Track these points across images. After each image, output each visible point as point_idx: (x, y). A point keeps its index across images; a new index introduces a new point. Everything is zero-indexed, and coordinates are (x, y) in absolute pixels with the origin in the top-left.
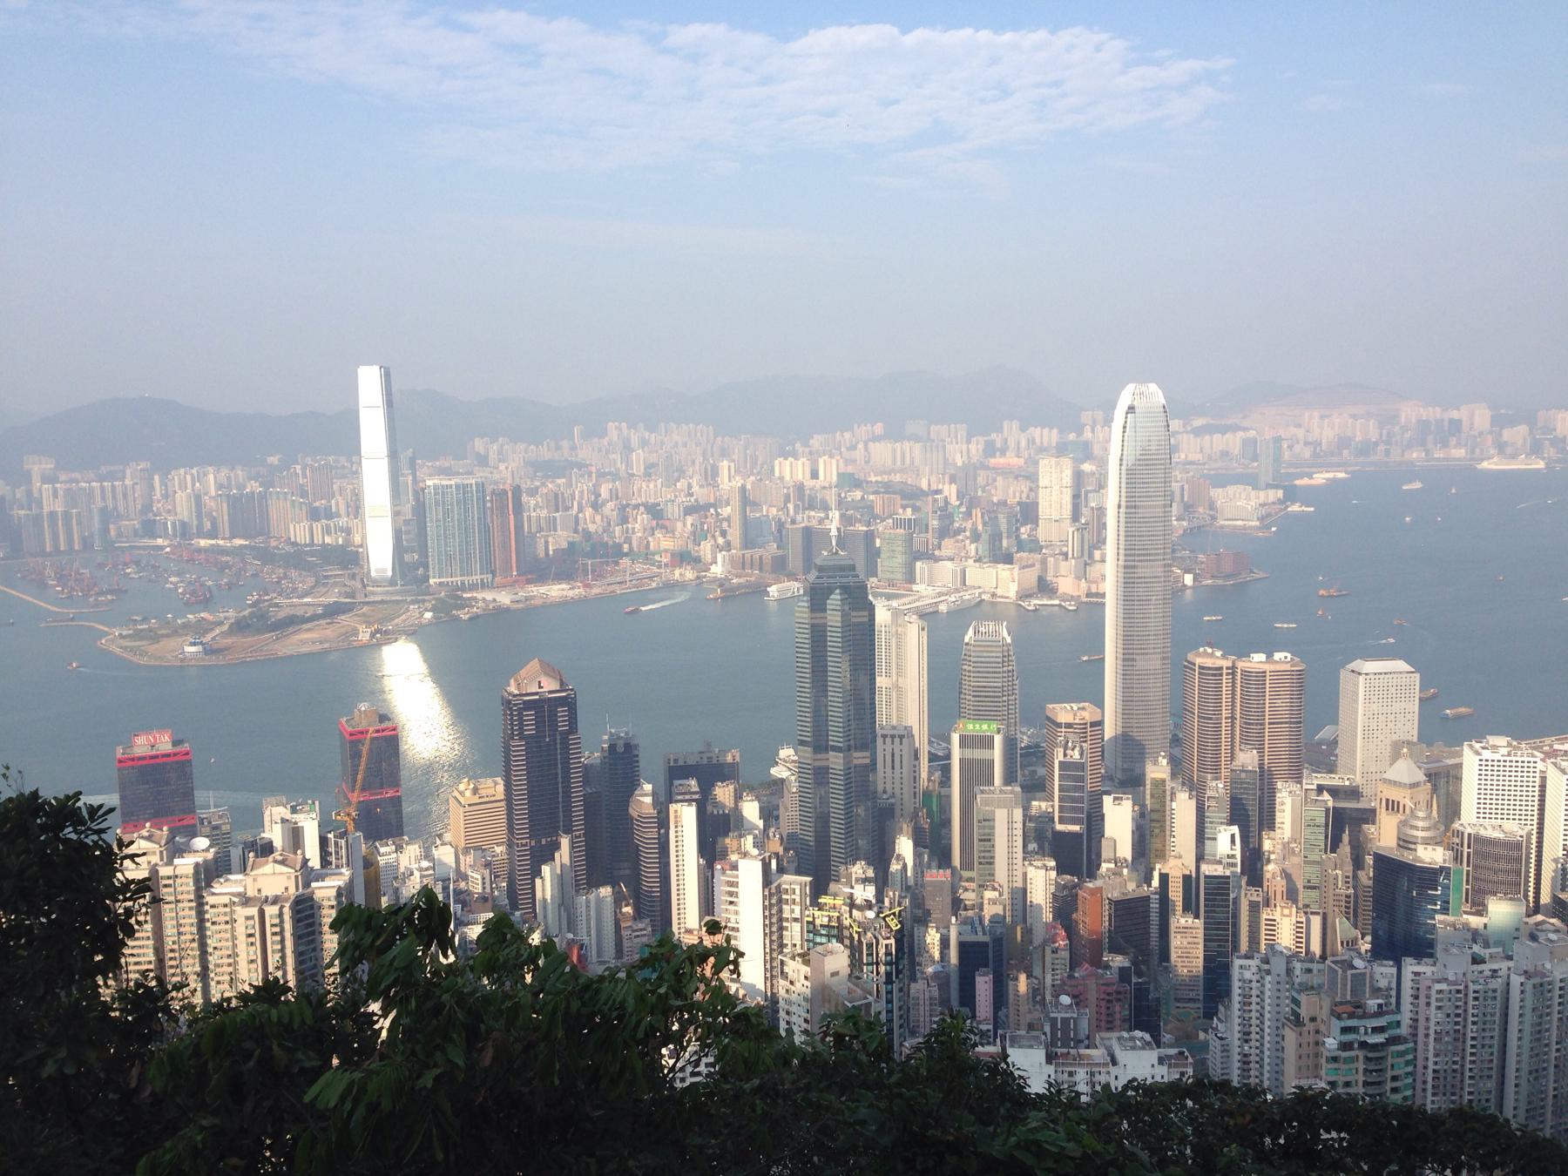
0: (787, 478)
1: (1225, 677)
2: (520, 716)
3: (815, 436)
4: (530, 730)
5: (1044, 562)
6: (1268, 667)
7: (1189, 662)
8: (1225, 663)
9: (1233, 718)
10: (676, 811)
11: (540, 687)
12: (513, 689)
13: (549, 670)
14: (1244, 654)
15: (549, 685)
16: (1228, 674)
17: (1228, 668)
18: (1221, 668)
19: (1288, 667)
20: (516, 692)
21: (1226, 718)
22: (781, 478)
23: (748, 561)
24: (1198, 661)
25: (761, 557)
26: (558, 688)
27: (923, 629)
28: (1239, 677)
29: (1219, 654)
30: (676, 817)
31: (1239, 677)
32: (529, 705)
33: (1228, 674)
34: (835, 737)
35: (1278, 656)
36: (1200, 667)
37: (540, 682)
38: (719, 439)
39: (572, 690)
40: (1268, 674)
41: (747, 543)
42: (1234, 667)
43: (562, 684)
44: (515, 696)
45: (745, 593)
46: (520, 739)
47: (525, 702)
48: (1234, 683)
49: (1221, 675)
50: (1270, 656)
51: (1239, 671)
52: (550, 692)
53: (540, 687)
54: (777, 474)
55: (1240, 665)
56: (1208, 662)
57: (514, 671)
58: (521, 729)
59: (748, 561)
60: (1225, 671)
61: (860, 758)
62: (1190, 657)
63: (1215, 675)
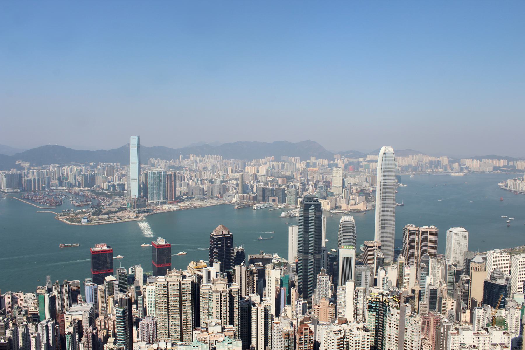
0: (249, 172)
1: (416, 233)
3: (254, 160)
4: (219, 246)
5: (336, 200)
6: (429, 230)
7: (405, 228)
8: (416, 229)
9: (418, 245)
10: (269, 271)
11: (223, 233)
12: (214, 233)
13: (225, 228)
14: (422, 226)
15: (225, 233)
16: (417, 232)
17: (417, 230)
19: (434, 230)
20: (215, 234)
21: (416, 245)
22: (248, 172)
23: (245, 198)
24: (409, 228)
25: (249, 196)
26: (228, 233)
27: (325, 218)
28: (420, 233)
29: (414, 226)
30: (269, 273)
31: (420, 233)
33: (417, 232)
34: (311, 249)
36: (409, 230)
37: (222, 232)
38: (224, 160)
39: (232, 234)
40: (429, 232)
41: (244, 192)
42: (419, 230)
43: (229, 233)
44: (215, 236)
45: (242, 208)
46: (217, 249)
47: (218, 238)
48: (419, 235)
49: (415, 232)
50: (429, 226)
51: (420, 231)
52: (226, 235)
53: (223, 233)
54: (246, 171)
56: (411, 228)
57: (214, 228)
58: (217, 246)
59: (245, 198)
60: (416, 231)
61: (318, 256)
62: (406, 227)
63: (413, 232)
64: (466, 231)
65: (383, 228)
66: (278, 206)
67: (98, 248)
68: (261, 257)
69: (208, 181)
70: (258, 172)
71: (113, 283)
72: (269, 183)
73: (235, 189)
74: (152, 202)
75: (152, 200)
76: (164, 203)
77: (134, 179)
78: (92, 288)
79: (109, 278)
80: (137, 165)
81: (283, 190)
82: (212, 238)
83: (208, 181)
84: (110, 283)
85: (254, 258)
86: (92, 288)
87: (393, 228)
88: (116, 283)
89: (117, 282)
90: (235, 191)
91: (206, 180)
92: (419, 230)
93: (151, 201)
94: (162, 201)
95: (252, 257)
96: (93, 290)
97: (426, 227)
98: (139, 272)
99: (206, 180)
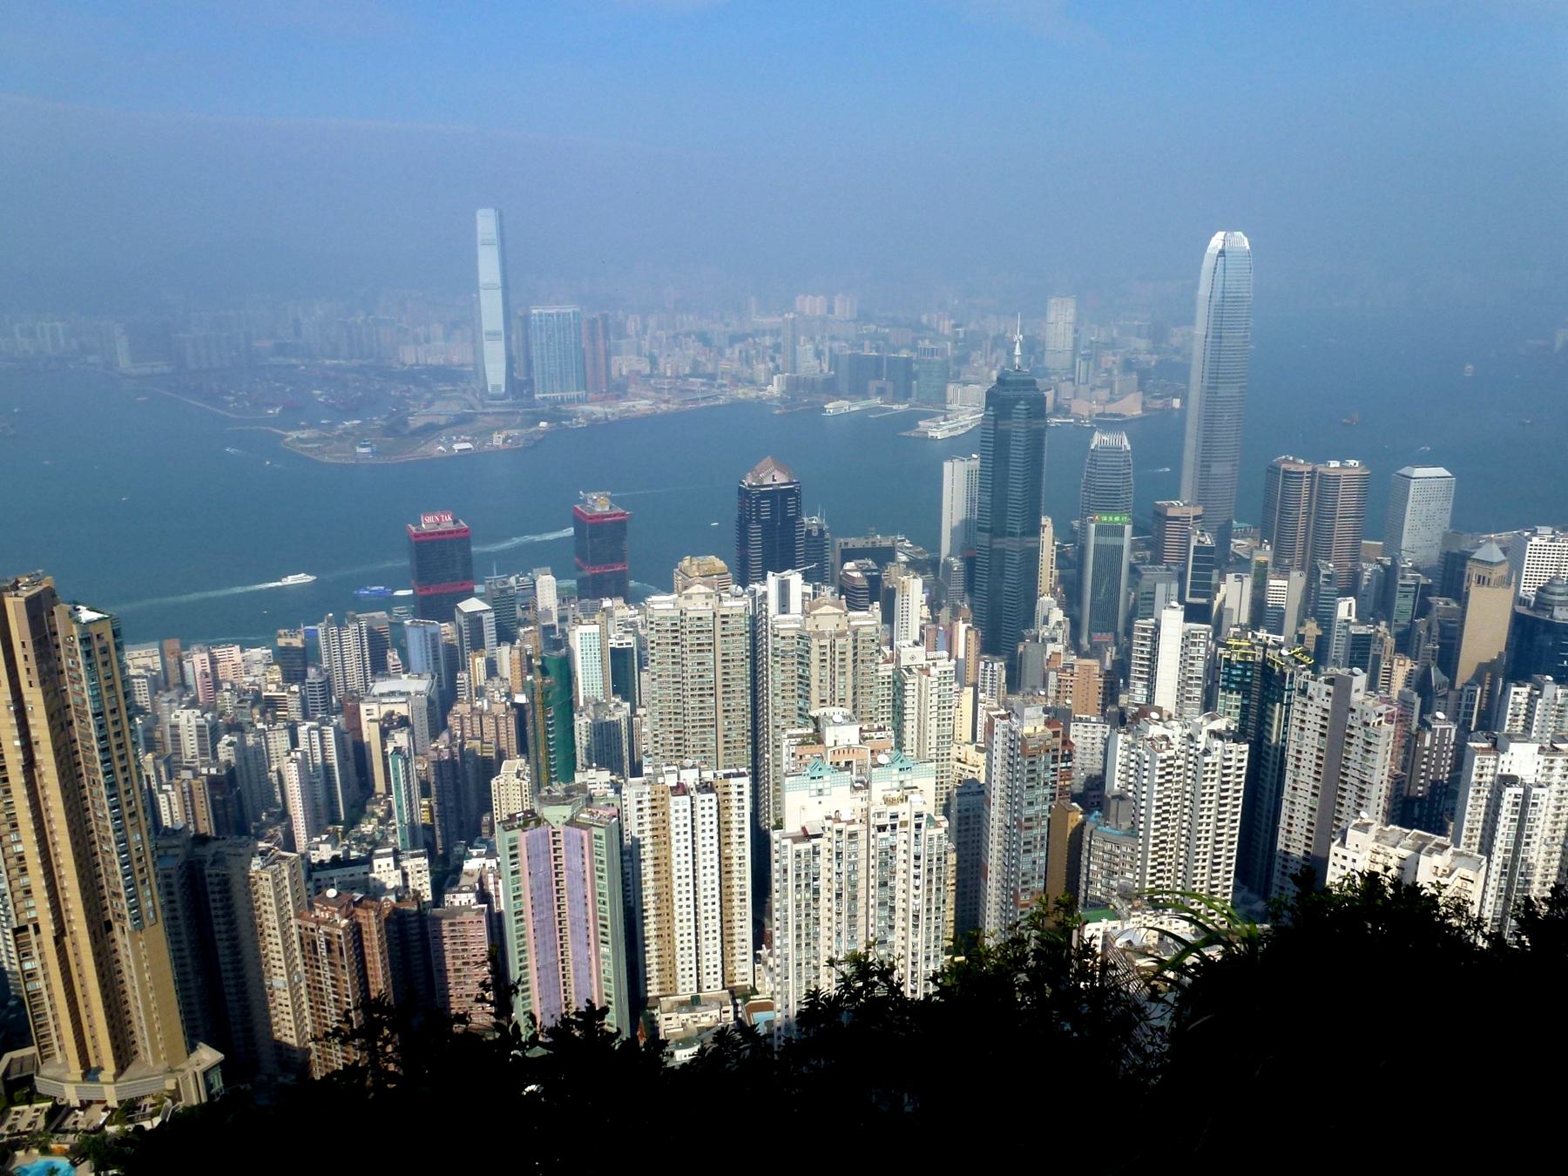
2: (758, 503)
4: (765, 516)
11: (774, 480)
12: (749, 481)
14: (1324, 461)
15: (781, 478)
17: (1308, 473)
18: (1303, 473)
19: (1357, 472)
31: (1317, 480)
32: (764, 495)
35: (1352, 462)
36: (1286, 471)
46: (758, 523)
49: (1302, 478)
53: (774, 480)
55: (1321, 468)
56: (1293, 468)
60: (1306, 475)
64: (1450, 475)
65: (1205, 465)
66: (895, 407)
67: (428, 523)
68: (870, 546)
69: (693, 337)
70: (831, 310)
71: (480, 619)
72: (867, 343)
73: (773, 359)
74: (544, 398)
75: (544, 392)
76: (580, 401)
77: (493, 335)
78: (425, 632)
79: (471, 605)
80: (499, 293)
81: (908, 361)
82: (744, 494)
83: (693, 337)
84: (475, 619)
85: (850, 546)
86: (425, 632)
87: (1233, 465)
88: (489, 620)
89: (492, 615)
90: (771, 365)
91: (688, 335)
92: (1314, 472)
93: (542, 395)
94: (573, 394)
95: (846, 544)
96: (429, 638)
97: (1335, 464)
98: (547, 590)
99: (688, 335)
